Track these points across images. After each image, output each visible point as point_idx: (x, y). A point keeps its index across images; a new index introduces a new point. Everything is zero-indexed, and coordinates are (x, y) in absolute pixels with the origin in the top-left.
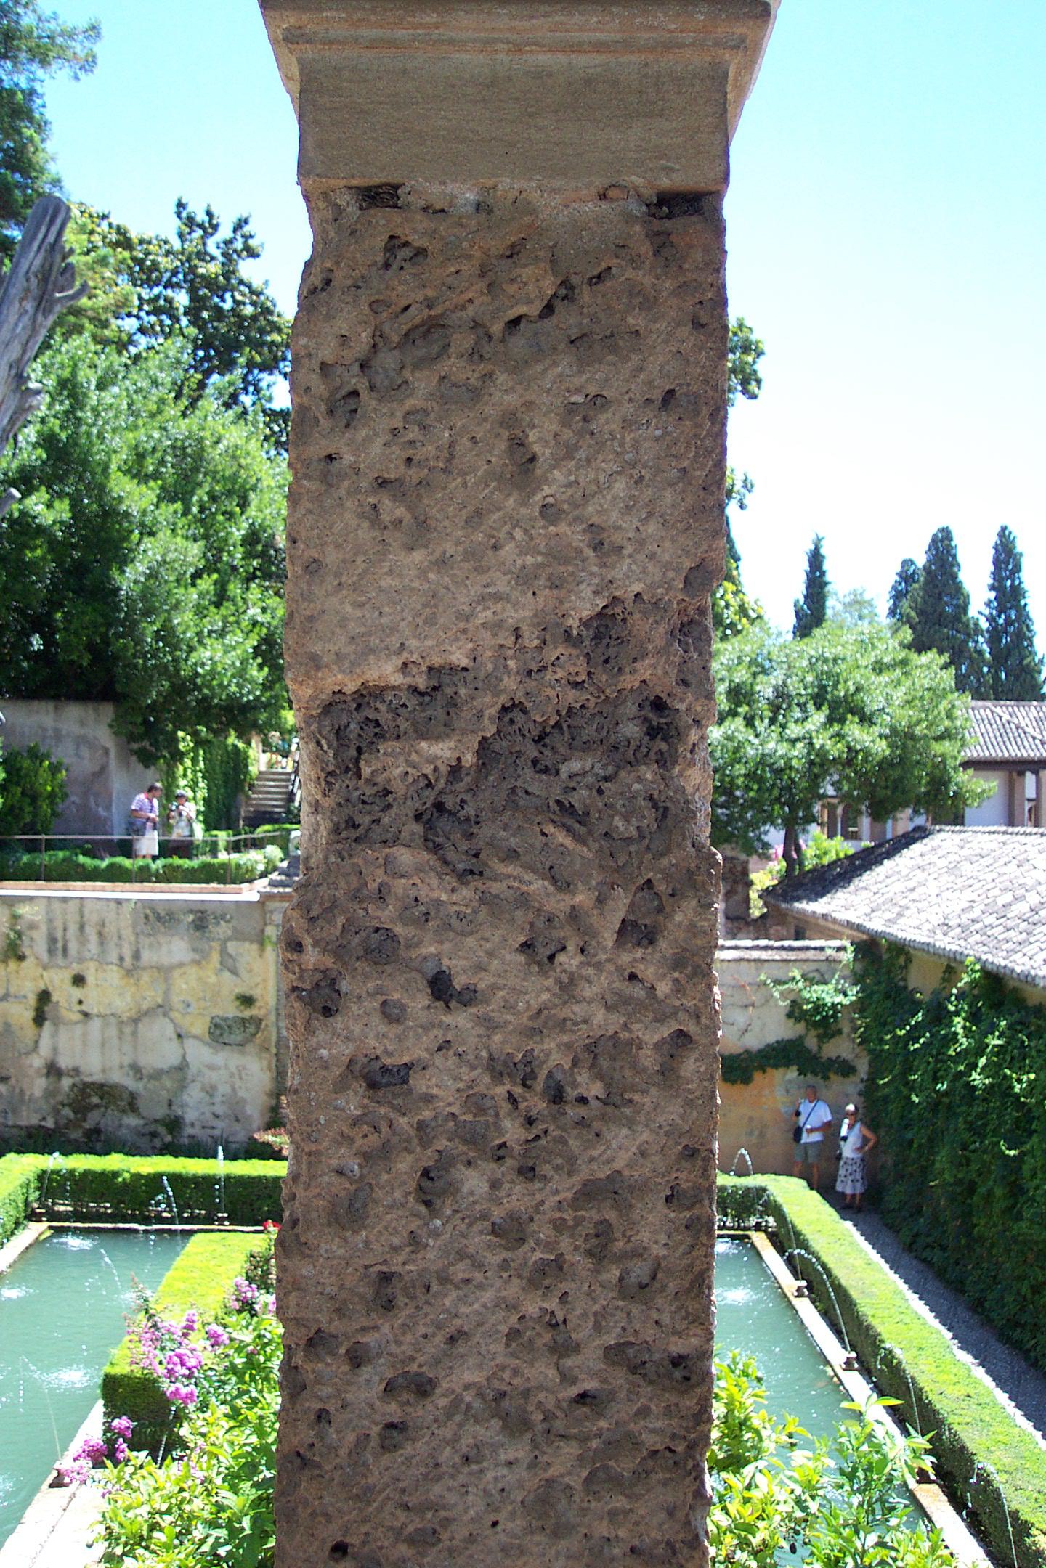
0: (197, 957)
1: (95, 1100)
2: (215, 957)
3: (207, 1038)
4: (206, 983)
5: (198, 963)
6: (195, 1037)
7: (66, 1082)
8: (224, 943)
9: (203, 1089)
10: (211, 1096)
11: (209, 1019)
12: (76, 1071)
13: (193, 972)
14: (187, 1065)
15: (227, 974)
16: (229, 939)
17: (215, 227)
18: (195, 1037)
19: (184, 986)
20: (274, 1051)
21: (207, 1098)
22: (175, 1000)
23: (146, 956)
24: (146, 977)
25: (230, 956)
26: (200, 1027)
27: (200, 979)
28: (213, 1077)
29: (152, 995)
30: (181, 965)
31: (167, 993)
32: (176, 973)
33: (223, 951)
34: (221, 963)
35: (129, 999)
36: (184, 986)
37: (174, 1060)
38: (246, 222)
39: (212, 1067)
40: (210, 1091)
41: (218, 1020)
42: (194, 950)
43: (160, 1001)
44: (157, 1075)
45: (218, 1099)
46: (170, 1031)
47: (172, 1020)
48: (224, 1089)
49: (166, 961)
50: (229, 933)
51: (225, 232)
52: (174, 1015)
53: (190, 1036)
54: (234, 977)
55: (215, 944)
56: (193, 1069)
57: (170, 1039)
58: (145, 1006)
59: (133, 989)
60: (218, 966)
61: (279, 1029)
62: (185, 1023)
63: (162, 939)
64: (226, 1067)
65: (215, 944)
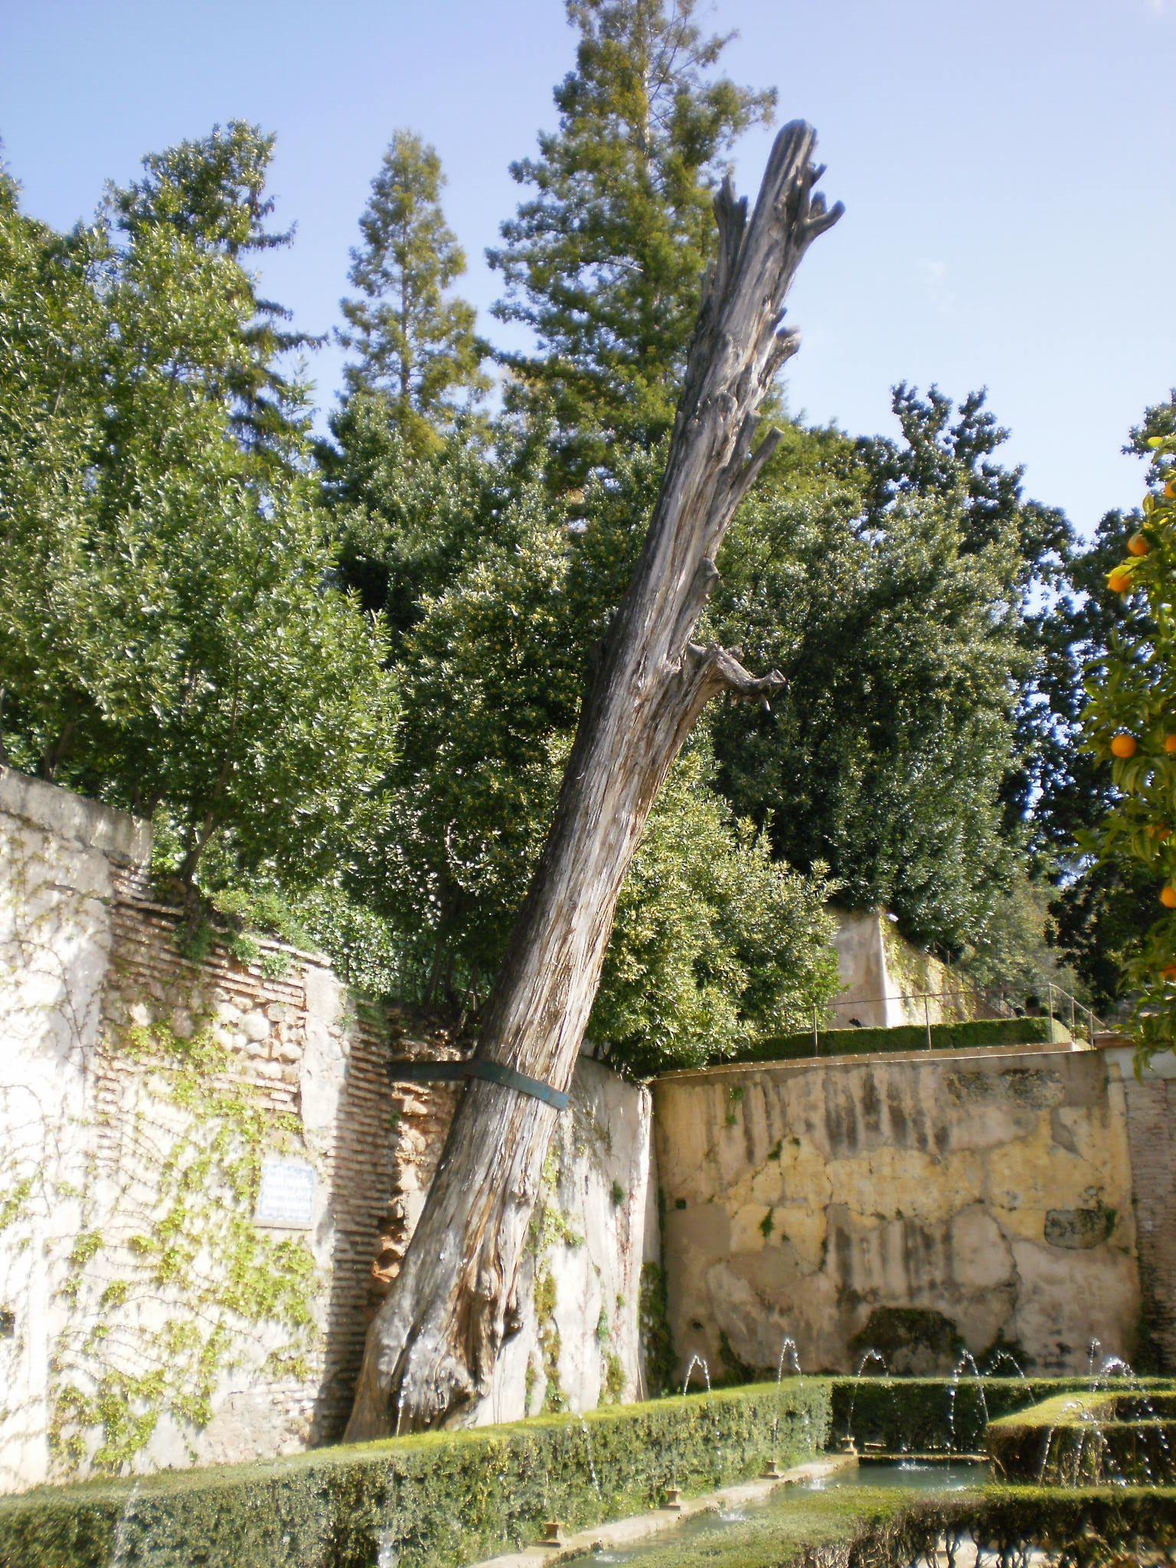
0: (1021, 1133)
1: (902, 1332)
2: (1045, 1131)
3: (1043, 1240)
4: (1035, 1166)
5: (1022, 1140)
6: (1027, 1240)
8: (1054, 1110)
9: (1043, 1311)
10: (1055, 1320)
11: (1043, 1215)
12: (874, 1292)
13: (1017, 1152)
14: (1019, 1277)
15: (1061, 1153)
16: (1061, 1105)
17: (944, 414)
18: (1027, 1240)
19: (1007, 1172)
20: (1134, 1252)
21: (1050, 1324)
22: (997, 1192)
23: (956, 1136)
24: (955, 1162)
25: (1064, 1127)
26: (1031, 1225)
27: (1027, 1162)
28: (1057, 1293)
29: (966, 1187)
30: (1000, 1144)
31: (985, 1181)
32: (995, 1156)
33: (1055, 1123)
34: (1053, 1138)
35: (936, 1194)
36: (1007, 1172)
37: (1002, 1273)
38: (982, 397)
39: (1052, 1280)
40: (1052, 1313)
41: (1054, 1215)
42: (1018, 1122)
43: (976, 1193)
44: (980, 1296)
45: (1063, 1325)
46: (993, 1231)
47: (995, 1220)
48: (1070, 1308)
49: (981, 1141)
50: (1061, 1096)
51: (955, 419)
52: (997, 1211)
53: (1019, 1238)
54: (1071, 1156)
55: (1044, 1113)
56: (1025, 1287)
57: (994, 1245)
58: (958, 1201)
59: (942, 1179)
60: (1050, 1142)
61: (1138, 1221)
62: (1011, 1221)
63: (974, 1110)
64: (1072, 1279)
65: (1044, 1113)
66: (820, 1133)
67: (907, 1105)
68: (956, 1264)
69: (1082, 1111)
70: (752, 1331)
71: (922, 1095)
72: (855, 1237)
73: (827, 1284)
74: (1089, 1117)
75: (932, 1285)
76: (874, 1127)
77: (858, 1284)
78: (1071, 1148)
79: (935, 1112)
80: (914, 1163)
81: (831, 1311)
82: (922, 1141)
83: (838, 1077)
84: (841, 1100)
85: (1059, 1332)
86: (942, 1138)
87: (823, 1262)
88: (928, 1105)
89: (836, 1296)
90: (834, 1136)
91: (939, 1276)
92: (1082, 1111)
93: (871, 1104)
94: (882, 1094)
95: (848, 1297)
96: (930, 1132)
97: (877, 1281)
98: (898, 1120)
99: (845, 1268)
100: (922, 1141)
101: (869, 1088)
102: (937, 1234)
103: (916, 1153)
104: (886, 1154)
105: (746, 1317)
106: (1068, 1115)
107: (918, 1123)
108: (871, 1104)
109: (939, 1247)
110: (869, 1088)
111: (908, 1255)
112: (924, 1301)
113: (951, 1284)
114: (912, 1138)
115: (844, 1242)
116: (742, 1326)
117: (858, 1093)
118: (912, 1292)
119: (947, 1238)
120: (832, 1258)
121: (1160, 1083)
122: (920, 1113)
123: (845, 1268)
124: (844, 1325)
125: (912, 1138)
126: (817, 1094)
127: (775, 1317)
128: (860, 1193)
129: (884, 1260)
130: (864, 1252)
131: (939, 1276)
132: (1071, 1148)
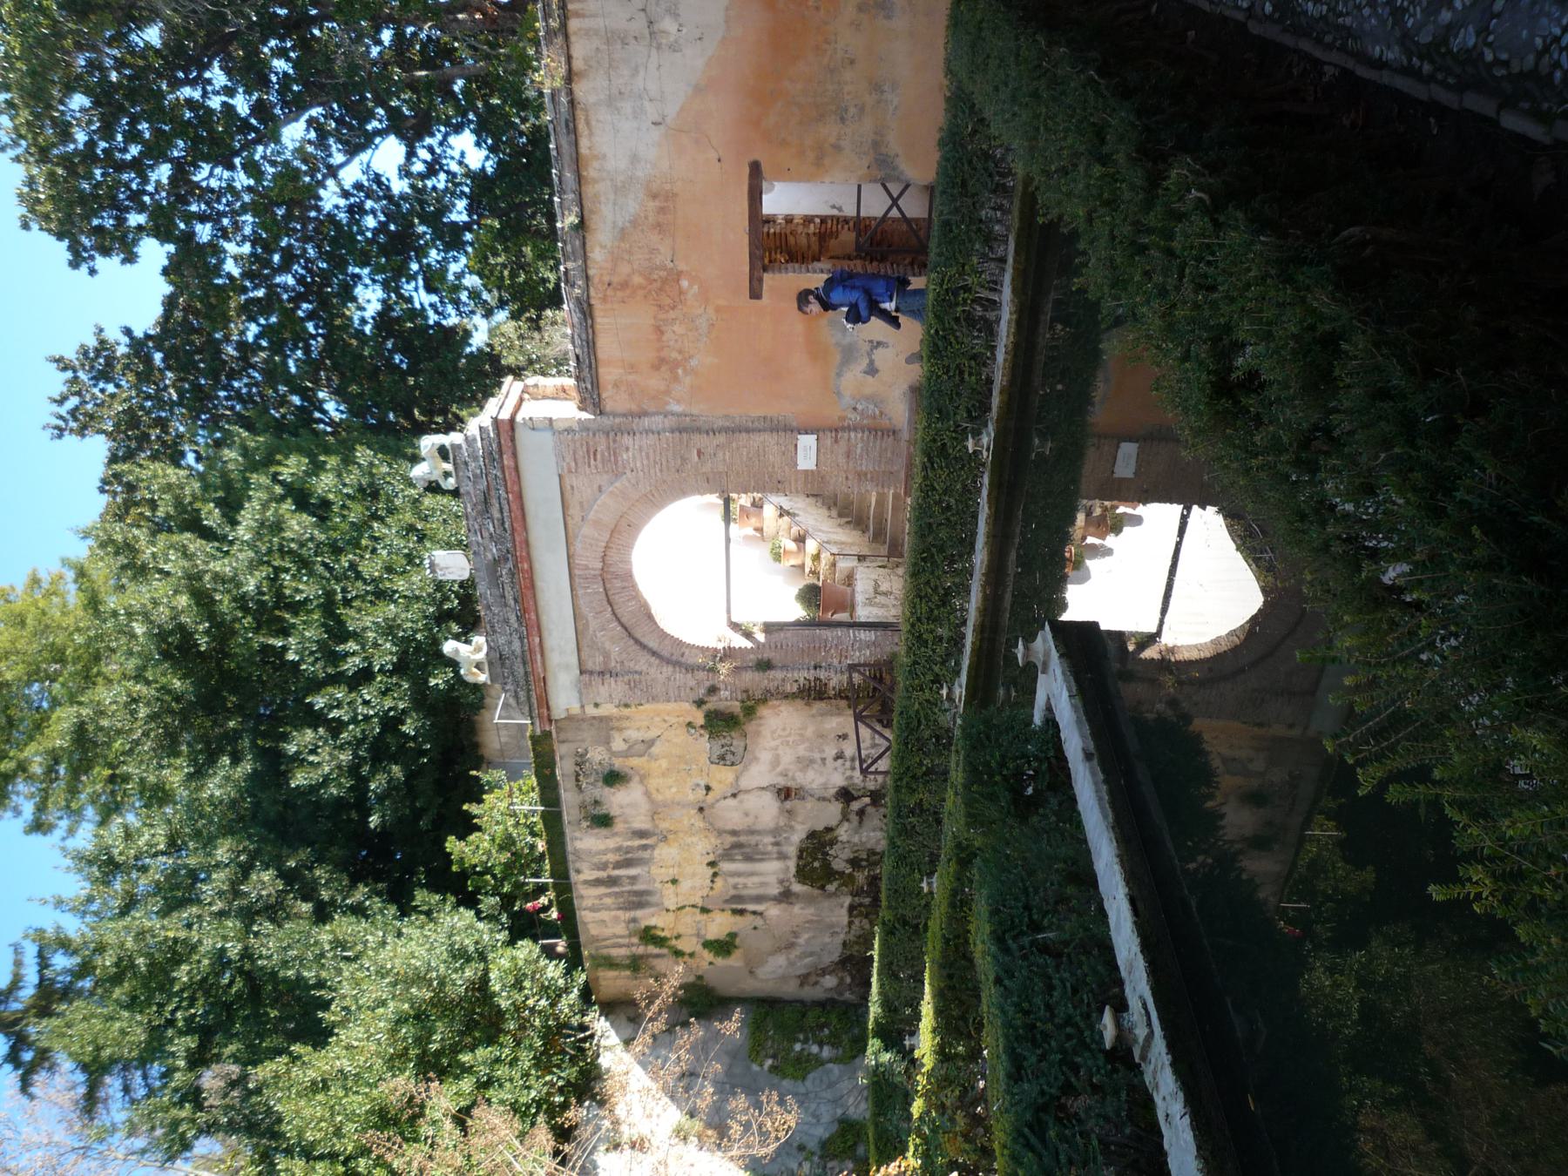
5: (643, 779)
7: (797, 888)
10: (812, 761)
12: (781, 882)
13: (653, 783)
23: (641, 823)
30: (647, 794)
33: (626, 754)
48: (802, 750)
49: (645, 806)
60: (645, 758)
66: (639, 913)
67: (612, 857)
68: (759, 827)
69: (615, 734)
70: (812, 954)
71: (602, 847)
72: (732, 892)
73: (773, 911)
74: (620, 730)
75: (777, 844)
76: (633, 879)
77: (775, 890)
78: (651, 743)
79: (618, 839)
80: (666, 854)
81: (797, 909)
82: (645, 847)
83: (588, 903)
84: (608, 901)
85: (823, 760)
86: (642, 834)
87: (754, 913)
88: (612, 843)
89: (783, 905)
90: (640, 905)
91: (769, 839)
92: (615, 734)
93: (612, 881)
94: (602, 874)
95: (786, 896)
96: (637, 842)
97: (772, 879)
98: (628, 863)
99: (759, 899)
100: (645, 847)
101: (598, 882)
102: (730, 839)
103: (656, 852)
104: (654, 870)
105: (800, 957)
106: (618, 744)
107: (629, 850)
108: (612, 881)
109: (743, 839)
110: (598, 882)
111: (748, 858)
112: (792, 851)
113: (776, 832)
114: (646, 854)
115: (738, 898)
116: (807, 960)
117: (602, 890)
118: (782, 857)
119: (734, 833)
120: (751, 907)
121: (586, 677)
122: (618, 849)
123: (759, 899)
124: (810, 900)
125: (641, 854)
126: (604, 915)
127: (801, 941)
128: (693, 888)
129: (752, 874)
130: (745, 886)
131: (769, 839)
132: (651, 743)
